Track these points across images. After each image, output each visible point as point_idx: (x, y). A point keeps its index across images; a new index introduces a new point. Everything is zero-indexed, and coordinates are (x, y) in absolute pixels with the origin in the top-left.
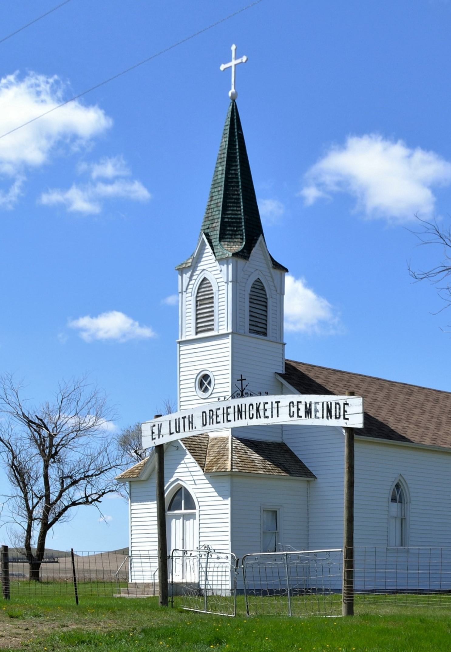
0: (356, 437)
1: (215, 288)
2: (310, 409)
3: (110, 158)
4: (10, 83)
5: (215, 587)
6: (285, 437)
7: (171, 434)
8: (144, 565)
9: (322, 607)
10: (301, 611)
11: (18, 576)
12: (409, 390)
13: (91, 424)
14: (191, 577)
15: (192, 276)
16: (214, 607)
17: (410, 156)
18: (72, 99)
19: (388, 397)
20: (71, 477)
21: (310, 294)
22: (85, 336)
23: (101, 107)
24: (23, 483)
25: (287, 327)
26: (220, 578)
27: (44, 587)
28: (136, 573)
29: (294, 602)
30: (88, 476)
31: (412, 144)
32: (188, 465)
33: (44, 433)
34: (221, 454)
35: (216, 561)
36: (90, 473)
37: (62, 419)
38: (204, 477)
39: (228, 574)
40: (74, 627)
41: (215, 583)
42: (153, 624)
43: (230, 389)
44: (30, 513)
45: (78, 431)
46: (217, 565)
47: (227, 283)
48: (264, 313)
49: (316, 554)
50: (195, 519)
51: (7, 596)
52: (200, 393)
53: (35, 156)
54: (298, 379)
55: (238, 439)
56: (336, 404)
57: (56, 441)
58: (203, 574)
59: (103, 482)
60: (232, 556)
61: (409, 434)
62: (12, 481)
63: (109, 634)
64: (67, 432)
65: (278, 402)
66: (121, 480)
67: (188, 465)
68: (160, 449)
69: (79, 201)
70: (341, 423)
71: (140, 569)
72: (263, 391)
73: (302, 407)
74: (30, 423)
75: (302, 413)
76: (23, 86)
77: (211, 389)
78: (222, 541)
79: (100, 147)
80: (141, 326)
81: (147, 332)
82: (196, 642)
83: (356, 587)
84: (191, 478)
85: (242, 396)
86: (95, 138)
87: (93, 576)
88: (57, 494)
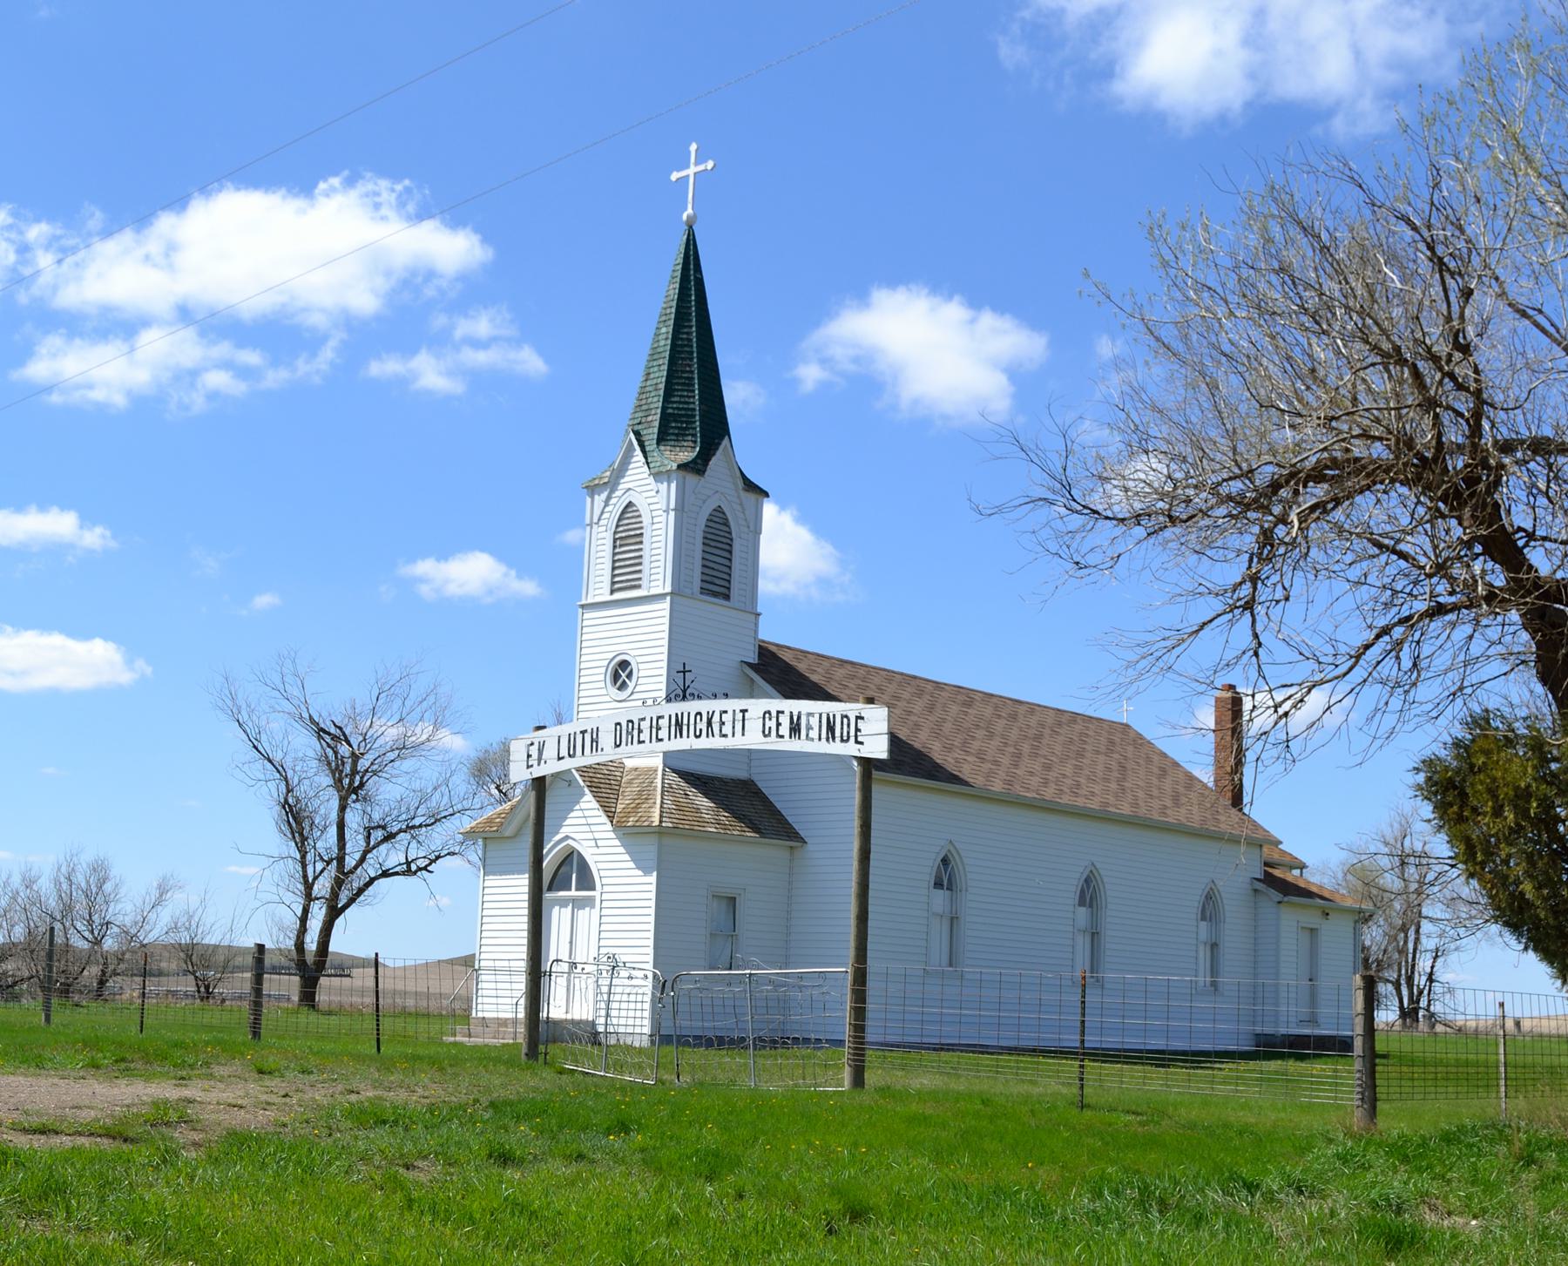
0: (876, 774)
1: (646, 520)
2: (798, 724)
3: (485, 307)
4: (333, 190)
5: (622, 1030)
6: (753, 770)
7: (560, 759)
8: (500, 986)
9: (809, 1071)
10: (772, 1078)
11: (279, 998)
12: (967, 697)
13: (424, 737)
14: (582, 1011)
15: (609, 498)
16: (620, 1067)
17: (973, 321)
18: (431, 216)
19: (931, 708)
20: (384, 828)
21: (804, 534)
22: (424, 589)
23: (476, 230)
24: (301, 834)
25: (764, 586)
26: (631, 1014)
27: (323, 1019)
28: (486, 1000)
29: (761, 1061)
30: (413, 827)
31: (977, 299)
32: (587, 813)
33: (344, 750)
34: (644, 796)
35: (626, 982)
36: (417, 822)
37: (375, 727)
38: (612, 835)
39: (647, 1006)
40: (370, 1094)
41: (622, 1021)
42: (509, 1094)
43: (663, 686)
44: (309, 887)
45: (403, 748)
46: (628, 990)
47: (667, 511)
48: (726, 562)
49: (801, 976)
50: (593, 907)
51: (256, 1034)
52: (613, 691)
53: (365, 301)
54: (780, 673)
55: (674, 771)
56: (843, 717)
57: (363, 764)
58: (603, 1005)
59: (437, 837)
60: (655, 975)
61: (966, 772)
62: (281, 831)
63: (431, 1109)
64: (382, 751)
65: (744, 711)
66: (470, 835)
67: (587, 813)
68: (539, 784)
69: (430, 374)
70: (851, 749)
71: (493, 993)
72: (720, 691)
73: (785, 720)
74: (320, 732)
75: (785, 730)
76: (354, 194)
77: (631, 685)
78: (639, 949)
79: (471, 291)
80: (520, 577)
81: (529, 588)
82: (584, 1129)
83: (871, 1035)
84: (590, 836)
85: (684, 698)
86: (463, 277)
87: (410, 1002)
88: (357, 856)
